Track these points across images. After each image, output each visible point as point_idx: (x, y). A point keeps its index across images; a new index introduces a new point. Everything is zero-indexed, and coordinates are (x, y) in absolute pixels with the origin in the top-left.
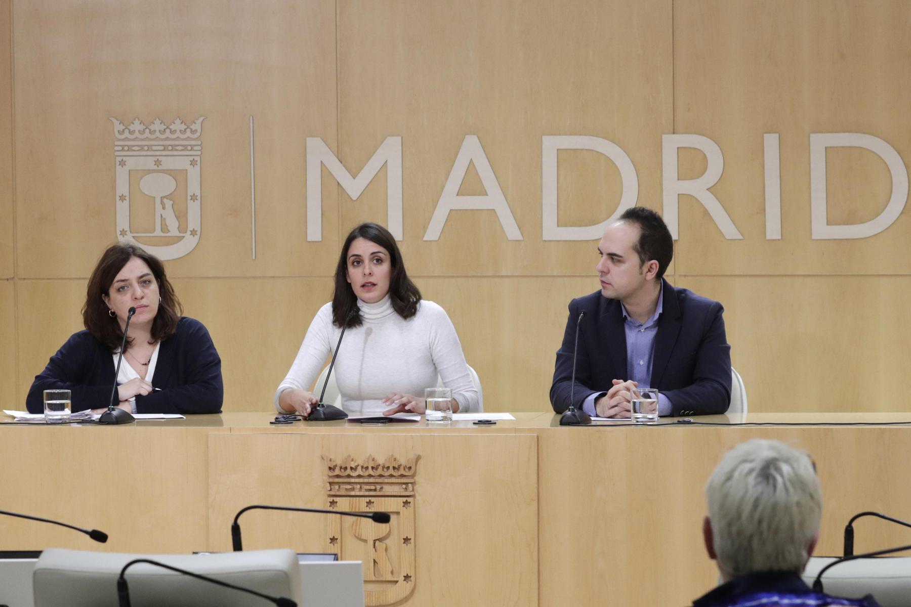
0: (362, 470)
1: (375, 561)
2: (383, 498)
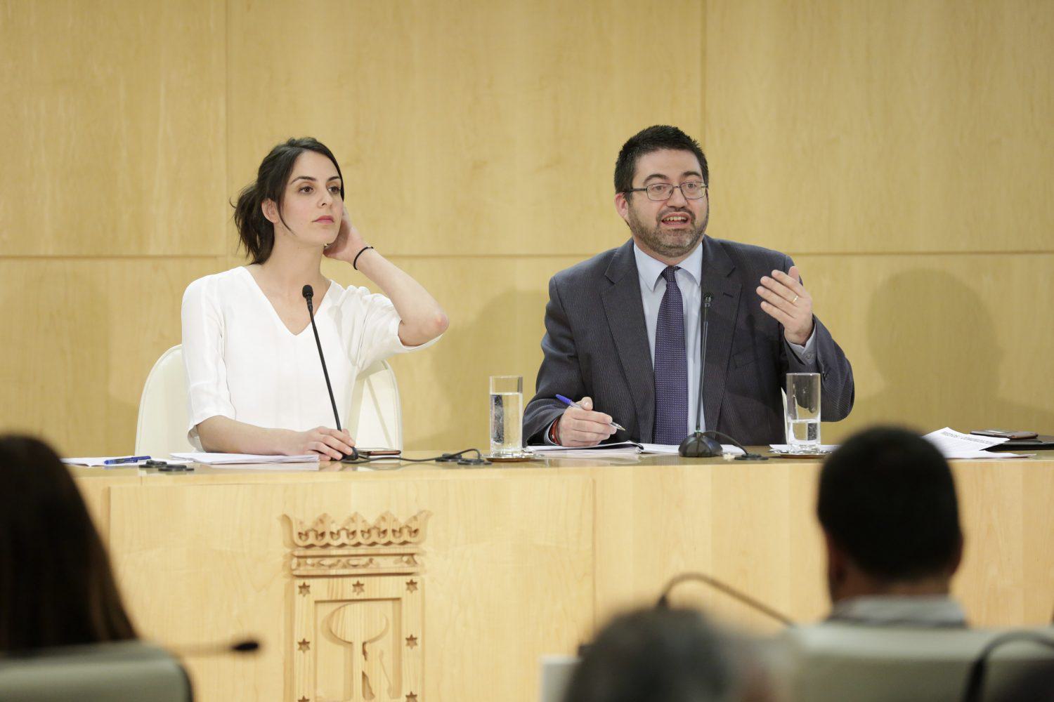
1: (364, 675)
2: (377, 578)
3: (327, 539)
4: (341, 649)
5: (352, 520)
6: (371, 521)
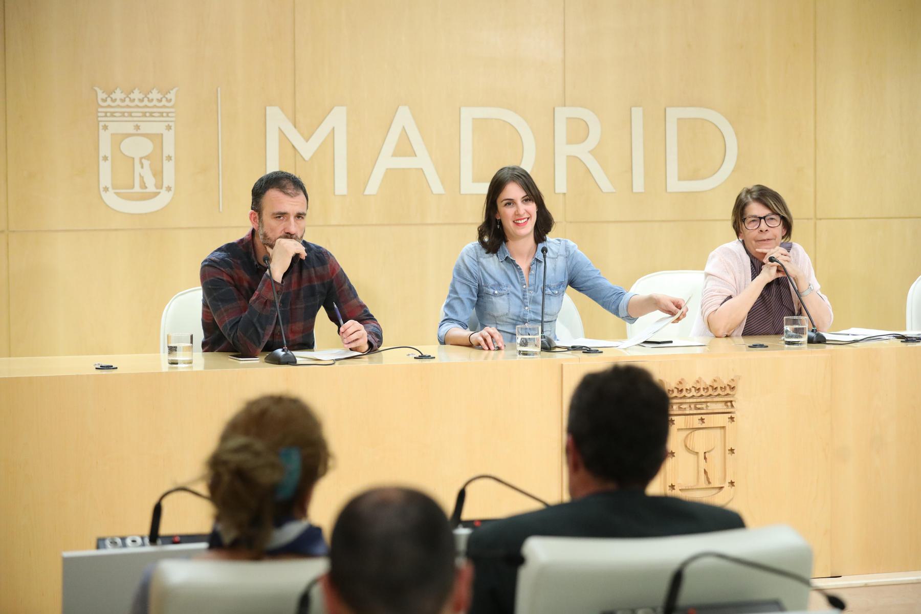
0: (695, 391)
1: (705, 471)
2: (712, 415)
3: (684, 393)
4: (692, 457)
5: (698, 382)
6: (709, 382)
